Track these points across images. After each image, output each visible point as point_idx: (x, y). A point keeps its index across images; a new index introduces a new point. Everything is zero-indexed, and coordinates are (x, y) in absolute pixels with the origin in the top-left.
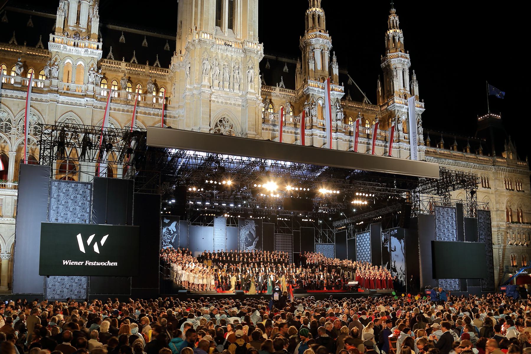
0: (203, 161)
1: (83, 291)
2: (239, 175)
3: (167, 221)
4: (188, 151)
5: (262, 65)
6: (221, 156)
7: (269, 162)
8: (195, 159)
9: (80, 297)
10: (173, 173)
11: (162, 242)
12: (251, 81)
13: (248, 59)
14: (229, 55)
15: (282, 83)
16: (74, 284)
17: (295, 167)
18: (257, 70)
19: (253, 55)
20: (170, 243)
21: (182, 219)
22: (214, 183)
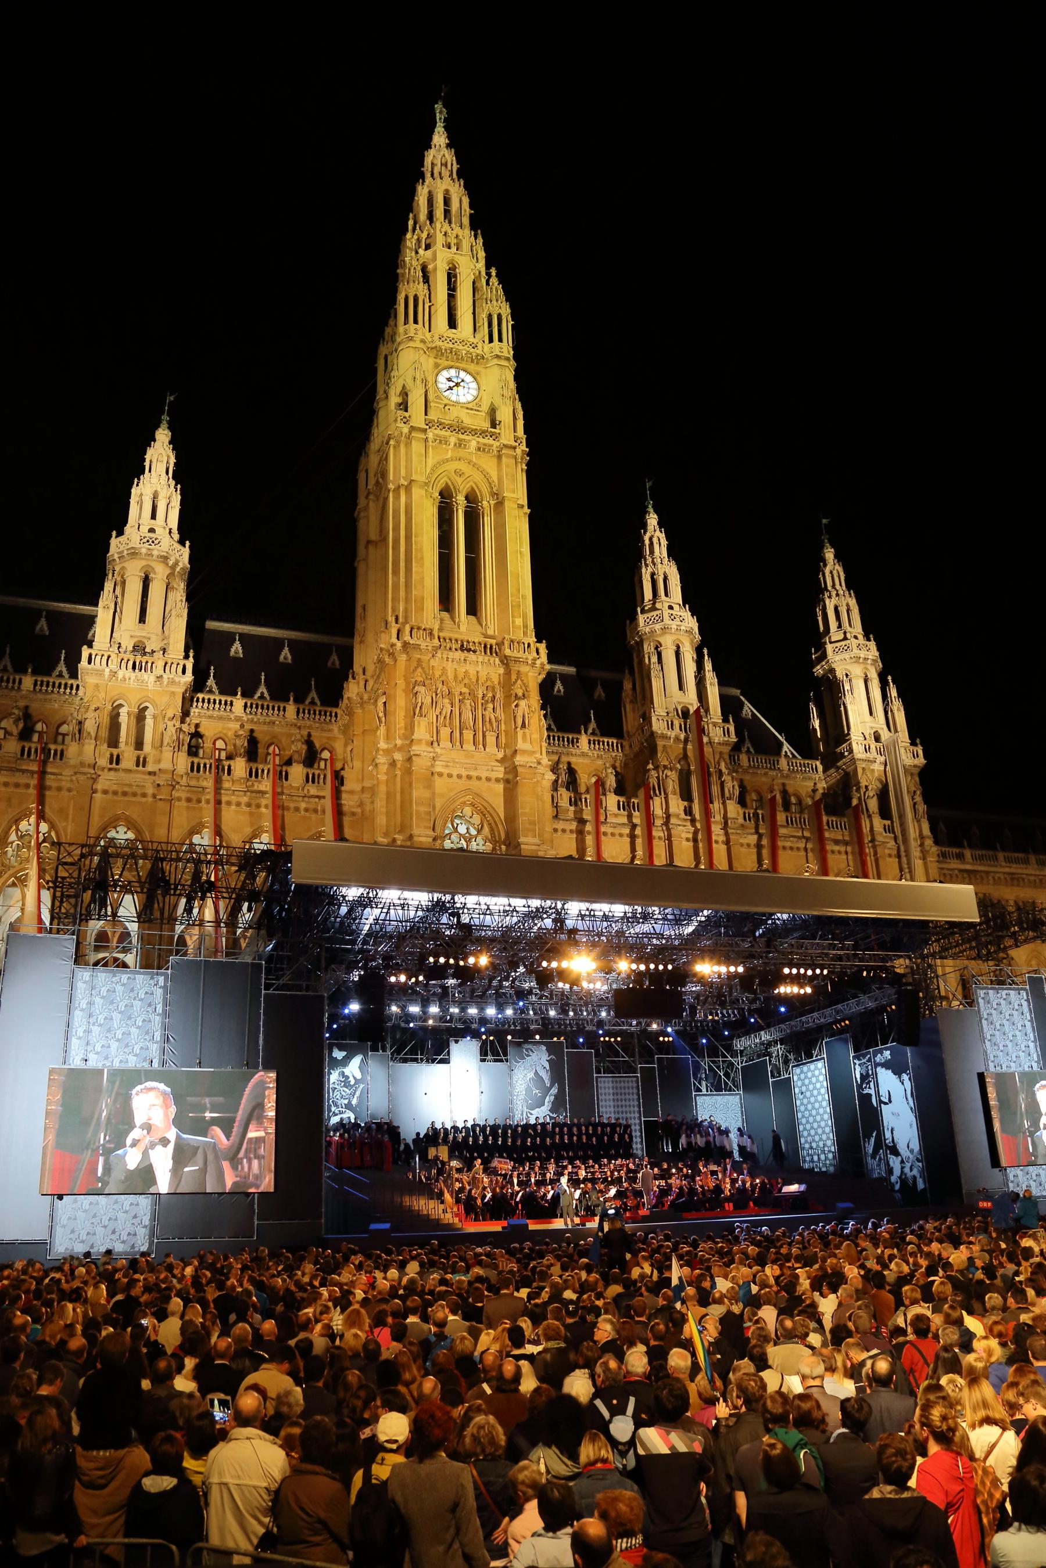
0: (420, 913)
1: (142, 1233)
2: (507, 942)
3: (338, 1054)
4: (386, 891)
5: (546, 687)
6: (462, 900)
7: (574, 907)
8: (403, 909)
9: (133, 1247)
10: (353, 942)
11: (329, 1106)
12: (523, 726)
13: (514, 677)
14: (472, 672)
15: (593, 725)
16: (120, 1215)
17: (634, 913)
18: (535, 699)
19: (524, 669)
20: (349, 1106)
21: (374, 1049)
22: (447, 962)
